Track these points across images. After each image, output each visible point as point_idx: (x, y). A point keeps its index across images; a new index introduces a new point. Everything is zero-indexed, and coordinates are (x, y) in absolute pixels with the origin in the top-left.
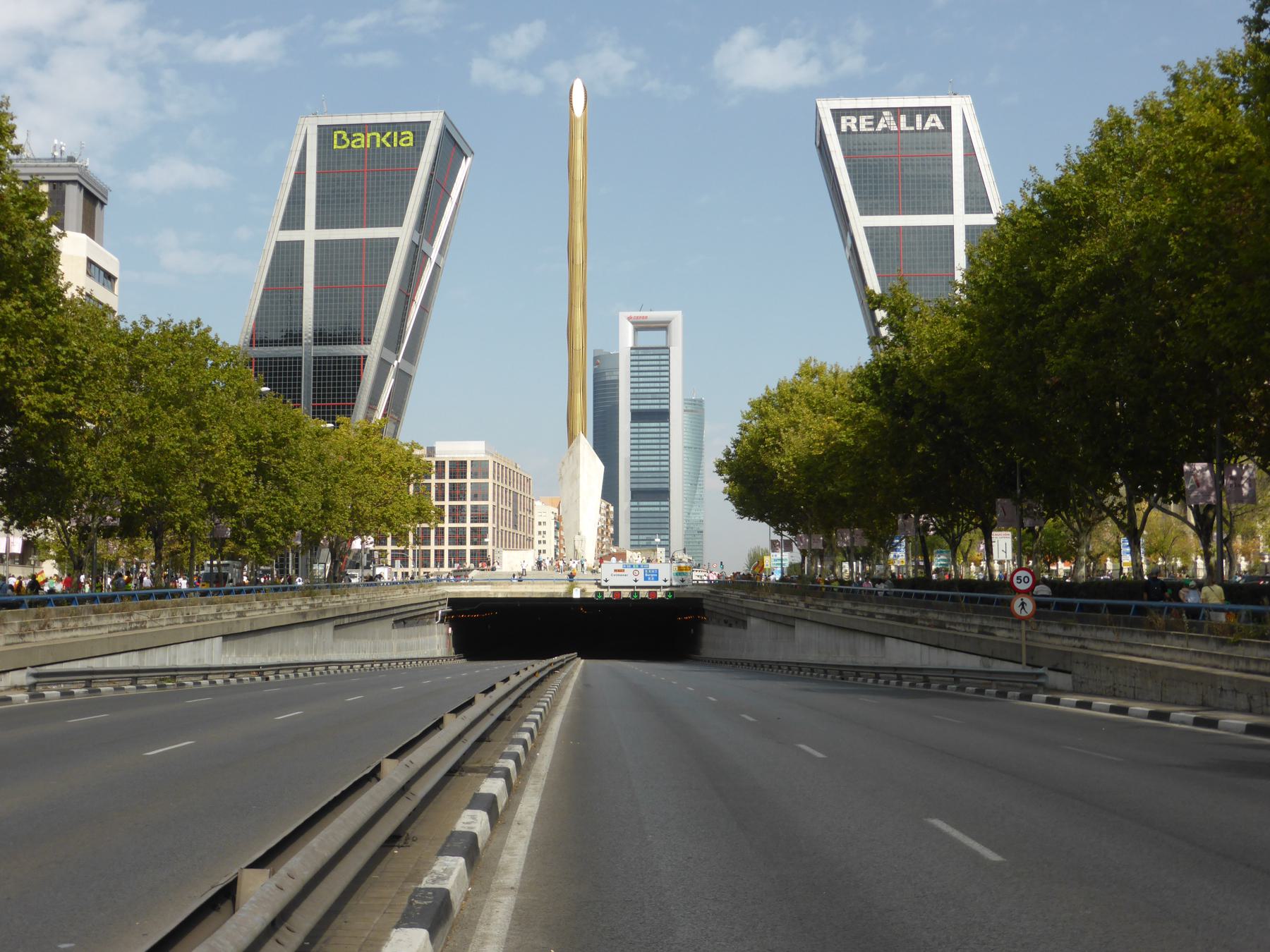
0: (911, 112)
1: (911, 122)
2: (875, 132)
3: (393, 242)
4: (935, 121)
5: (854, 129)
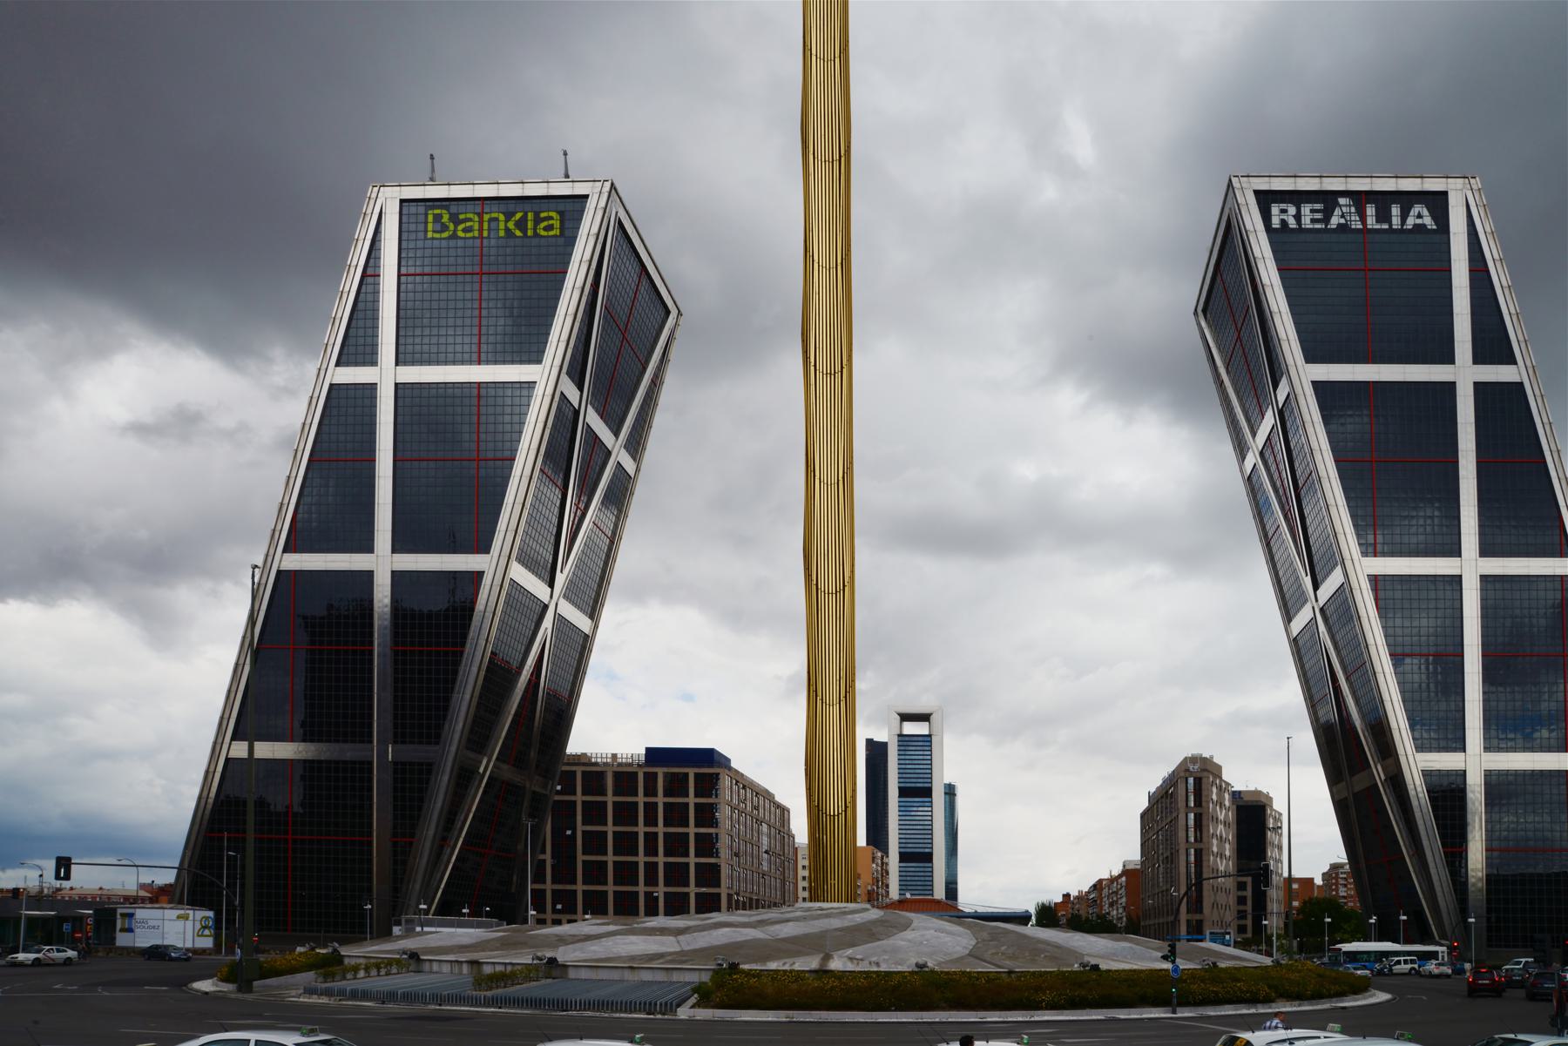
0: (1383, 200)
1: (1383, 216)
2: (1326, 230)
4: (1421, 216)
5: (1292, 223)
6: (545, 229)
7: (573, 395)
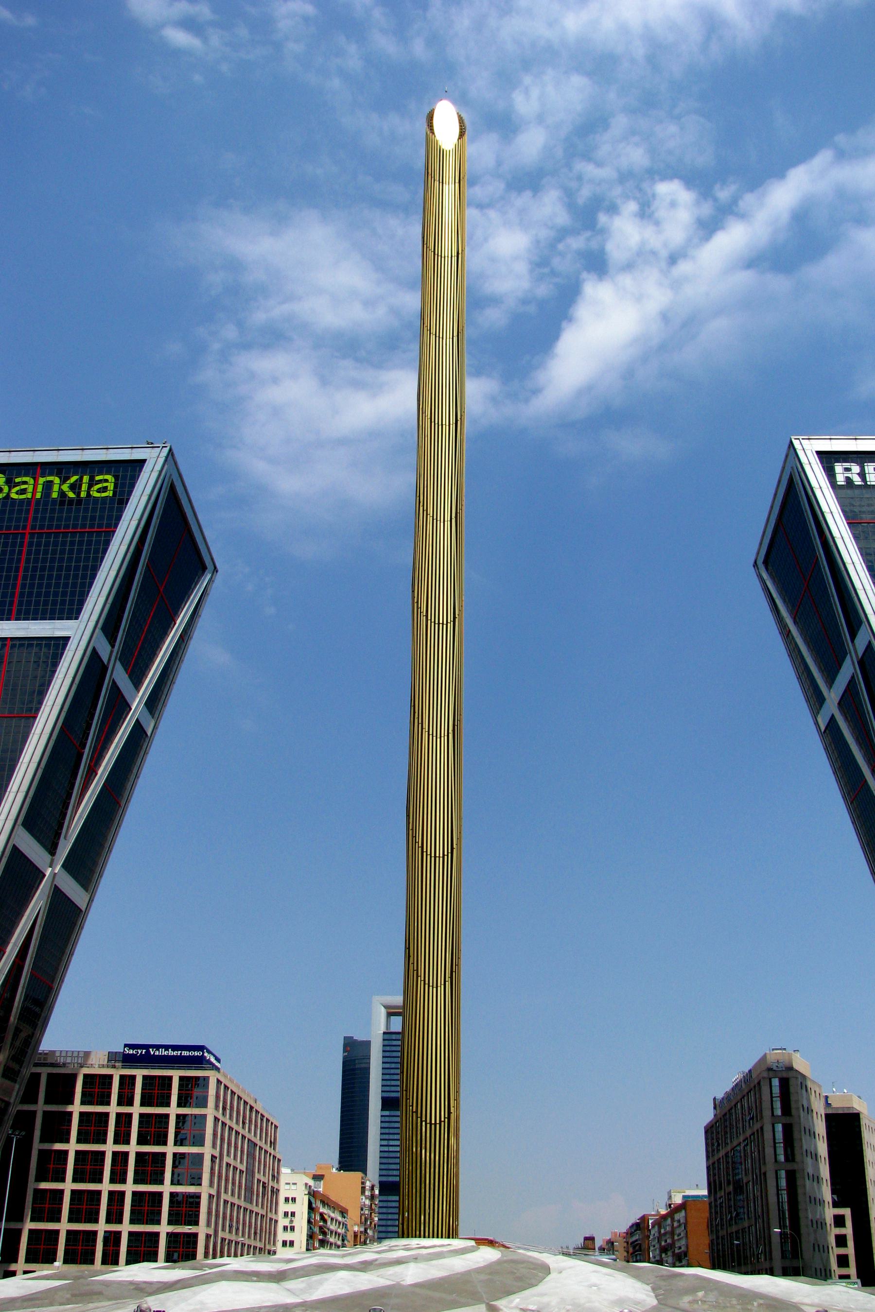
3: (60, 643)
6: (98, 491)
7: (104, 650)
